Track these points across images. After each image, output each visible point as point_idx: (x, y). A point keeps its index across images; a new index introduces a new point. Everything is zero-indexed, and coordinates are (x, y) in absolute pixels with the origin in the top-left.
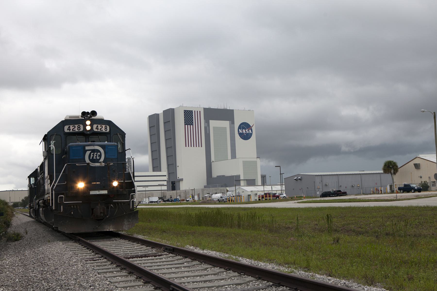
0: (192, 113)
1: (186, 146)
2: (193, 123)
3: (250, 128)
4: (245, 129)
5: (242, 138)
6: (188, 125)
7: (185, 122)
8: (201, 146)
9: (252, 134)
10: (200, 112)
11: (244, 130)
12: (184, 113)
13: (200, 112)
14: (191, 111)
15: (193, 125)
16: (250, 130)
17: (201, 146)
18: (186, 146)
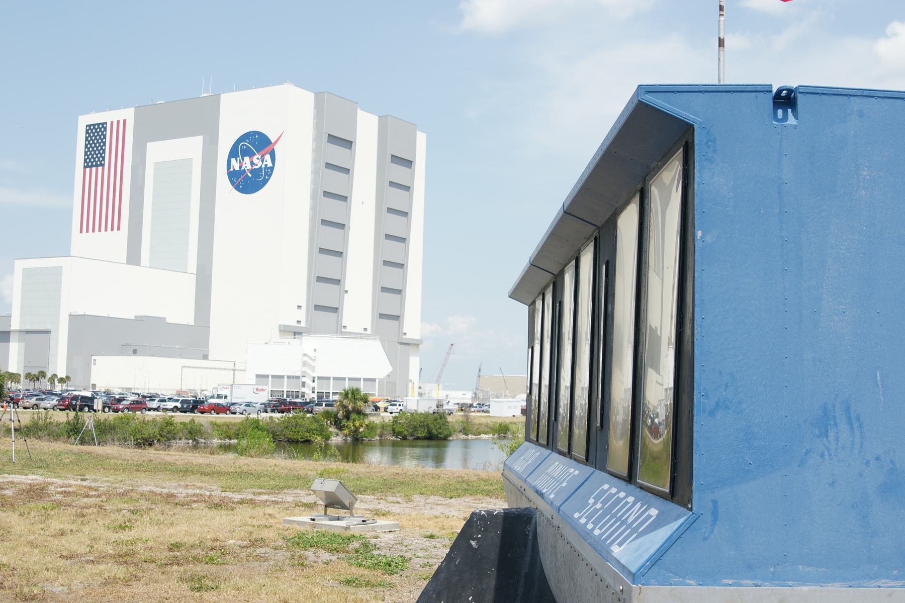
0: (105, 130)
1: (81, 232)
2: (104, 159)
3: (269, 148)
4: (251, 155)
5: (237, 188)
6: (92, 166)
7: (85, 161)
8: (119, 229)
9: (272, 169)
10: (125, 121)
11: (247, 159)
12: (87, 132)
13: (125, 121)
14: (103, 124)
15: (103, 165)
16: (268, 157)
17: (119, 229)
18: (81, 232)
